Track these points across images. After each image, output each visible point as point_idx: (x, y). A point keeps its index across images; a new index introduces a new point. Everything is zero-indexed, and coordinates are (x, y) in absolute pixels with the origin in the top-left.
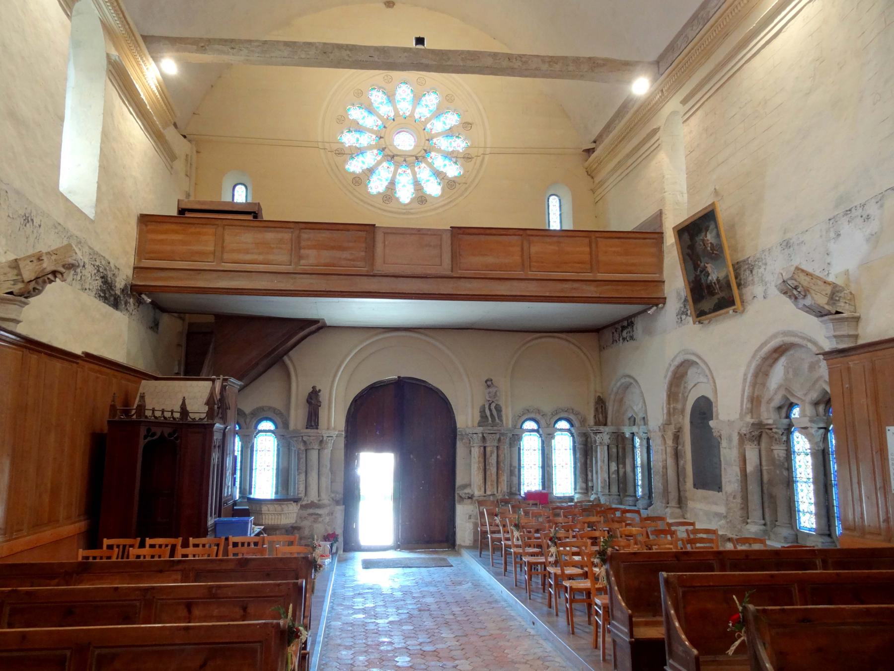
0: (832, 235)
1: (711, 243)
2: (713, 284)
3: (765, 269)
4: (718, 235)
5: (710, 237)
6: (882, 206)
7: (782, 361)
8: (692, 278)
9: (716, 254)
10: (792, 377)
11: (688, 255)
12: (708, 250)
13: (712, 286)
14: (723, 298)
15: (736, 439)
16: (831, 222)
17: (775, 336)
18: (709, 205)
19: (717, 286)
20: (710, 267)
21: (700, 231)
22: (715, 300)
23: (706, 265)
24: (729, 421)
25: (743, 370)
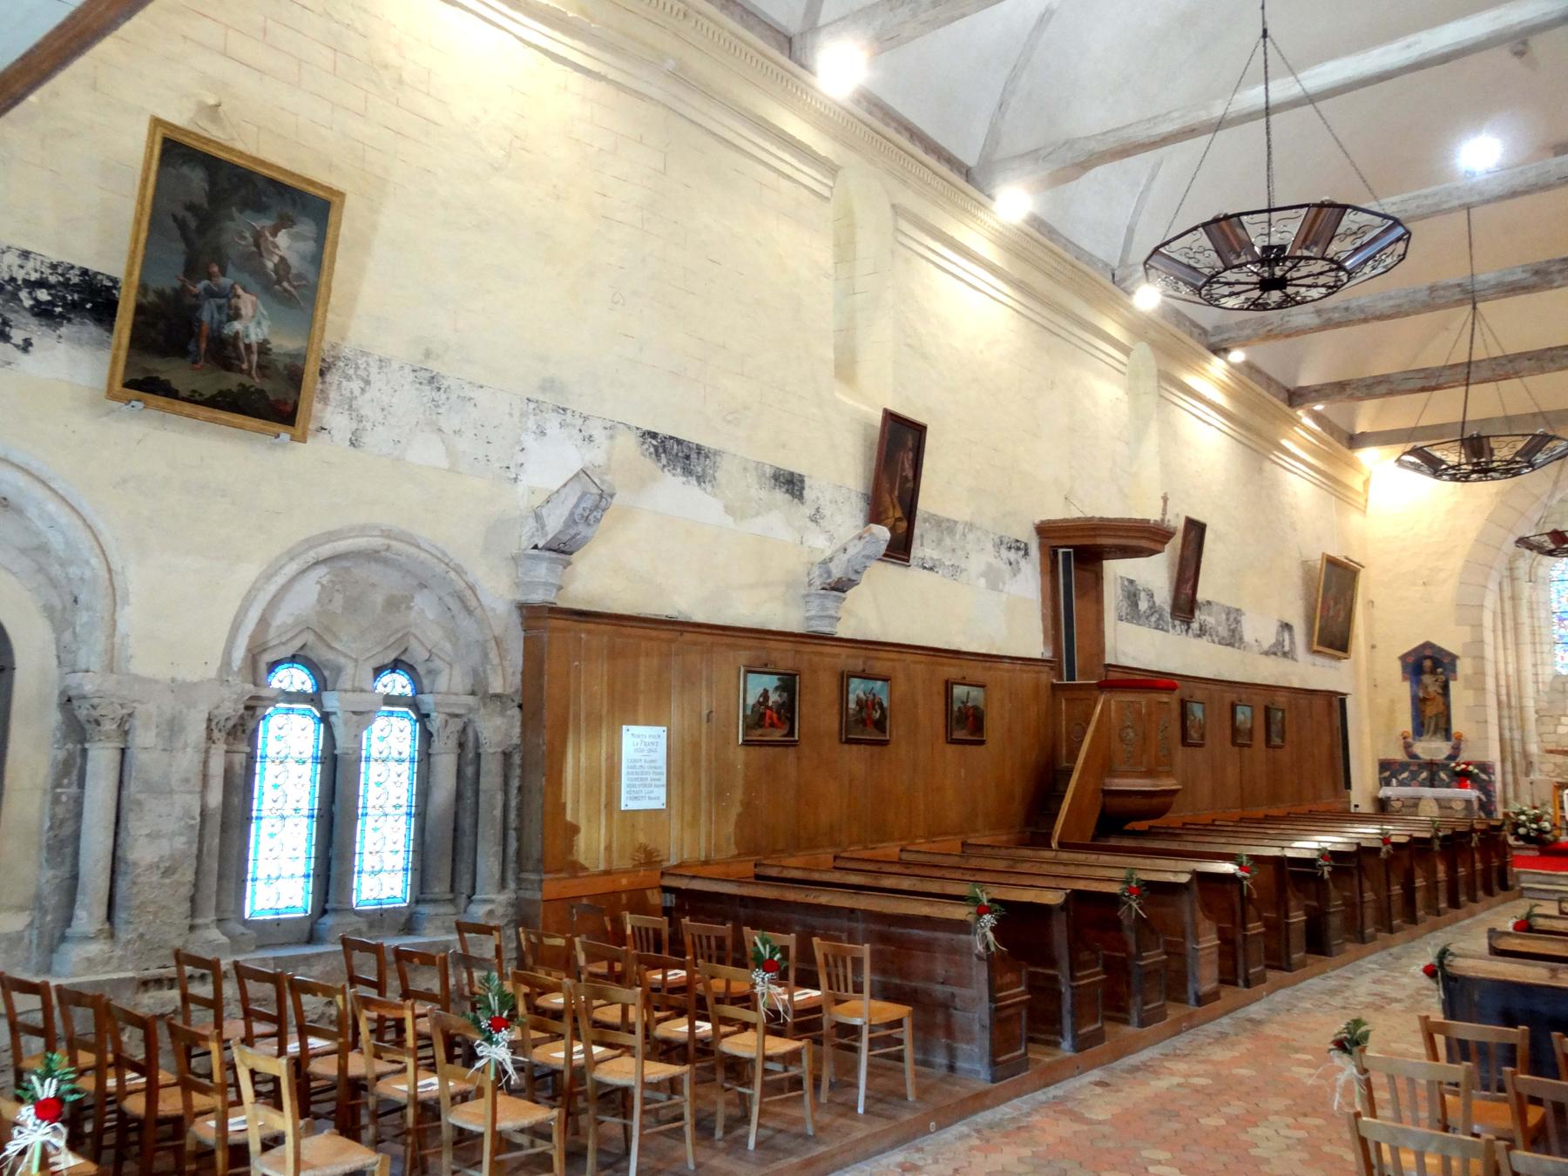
0: (531, 423)
1: (282, 259)
2: (242, 346)
3: (363, 390)
4: (318, 260)
5: (286, 245)
6: (612, 437)
7: (322, 571)
8: (169, 280)
9: (286, 290)
10: (339, 611)
11: (182, 225)
12: (264, 266)
13: (236, 347)
14: (261, 392)
15: (195, 731)
16: (532, 405)
17: (363, 530)
18: (329, 189)
19: (255, 358)
20: (247, 303)
21: (260, 208)
22: (232, 381)
23: (240, 291)
24: (173, 680)
25: (249, 572)
